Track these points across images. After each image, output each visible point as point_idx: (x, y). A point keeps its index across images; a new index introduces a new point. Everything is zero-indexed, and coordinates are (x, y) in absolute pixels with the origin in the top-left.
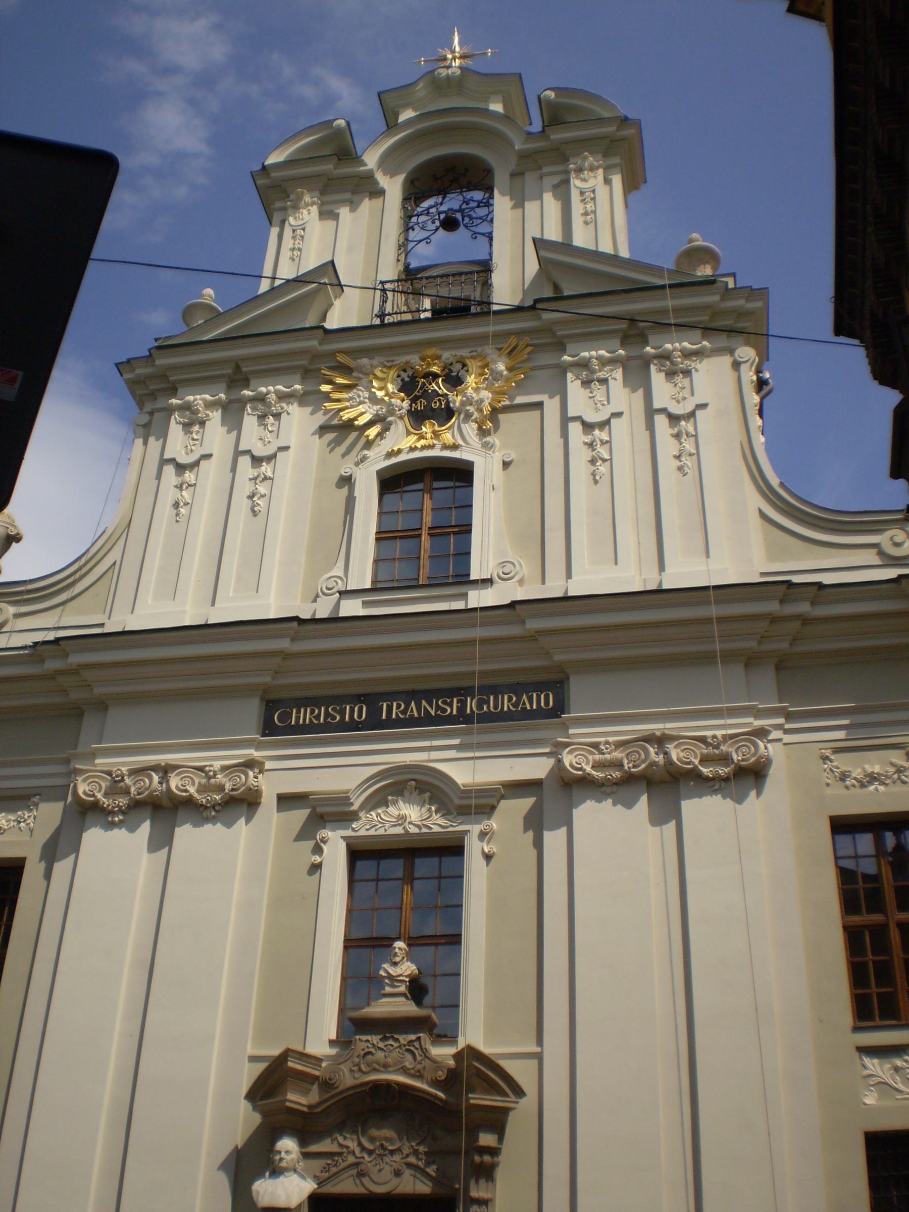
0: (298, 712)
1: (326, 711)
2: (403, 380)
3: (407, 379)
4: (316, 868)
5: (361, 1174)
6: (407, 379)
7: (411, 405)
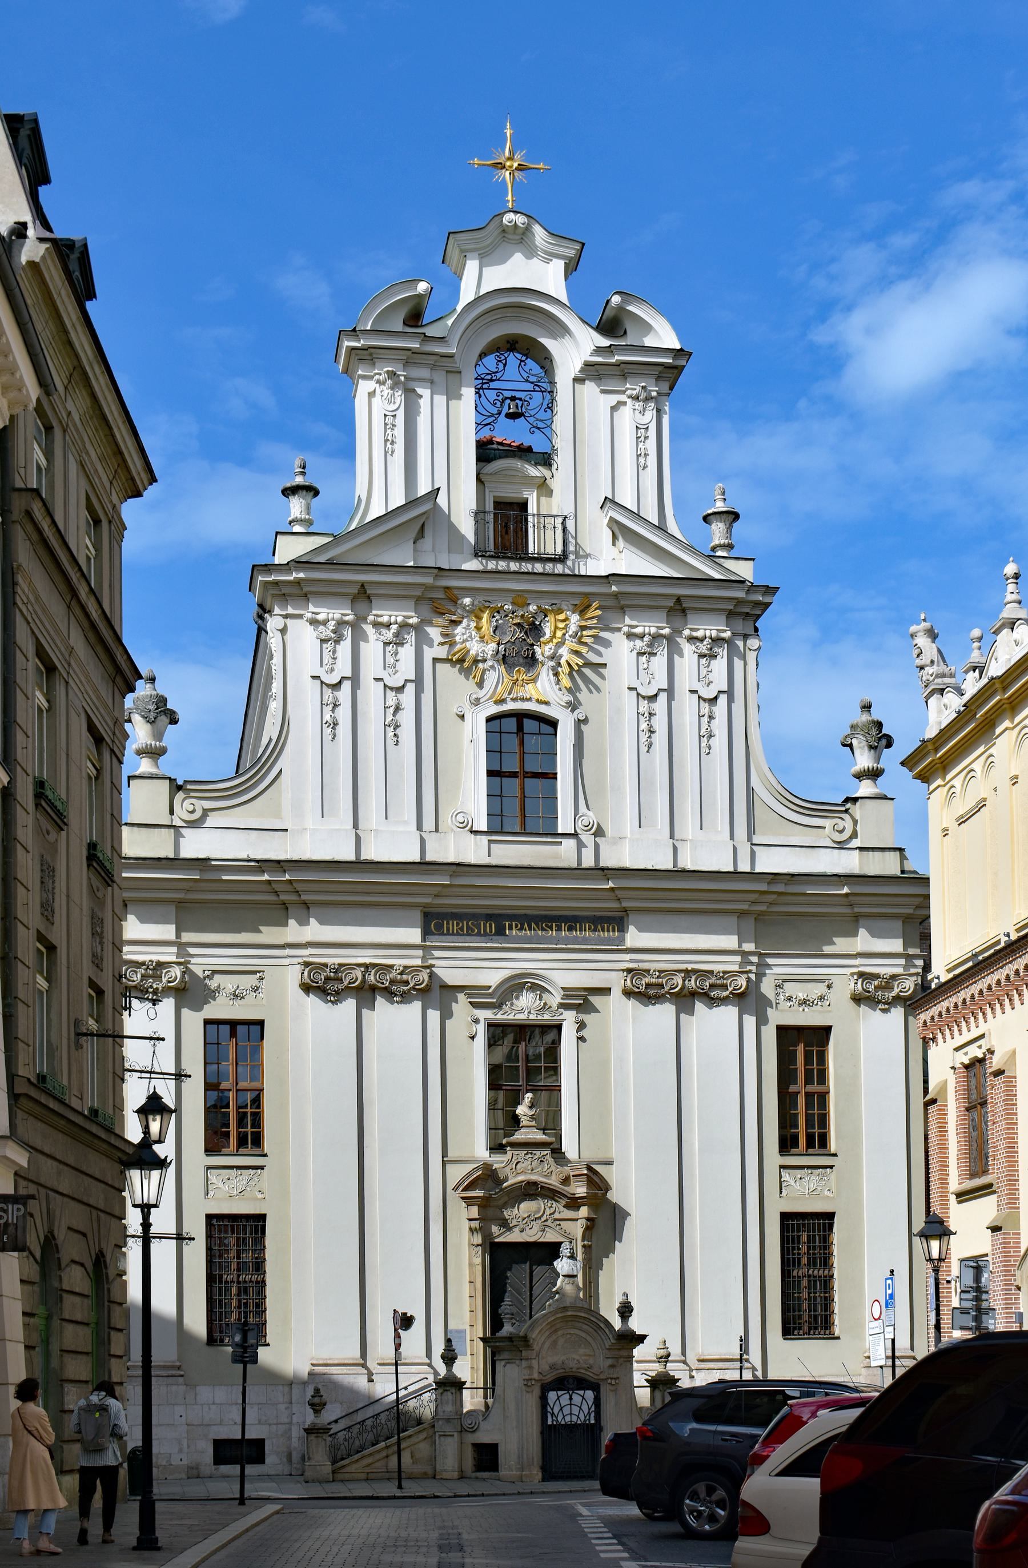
0: (448, 924)
1: (467, 924)
4: (473, 1038)
7: (505, 650)
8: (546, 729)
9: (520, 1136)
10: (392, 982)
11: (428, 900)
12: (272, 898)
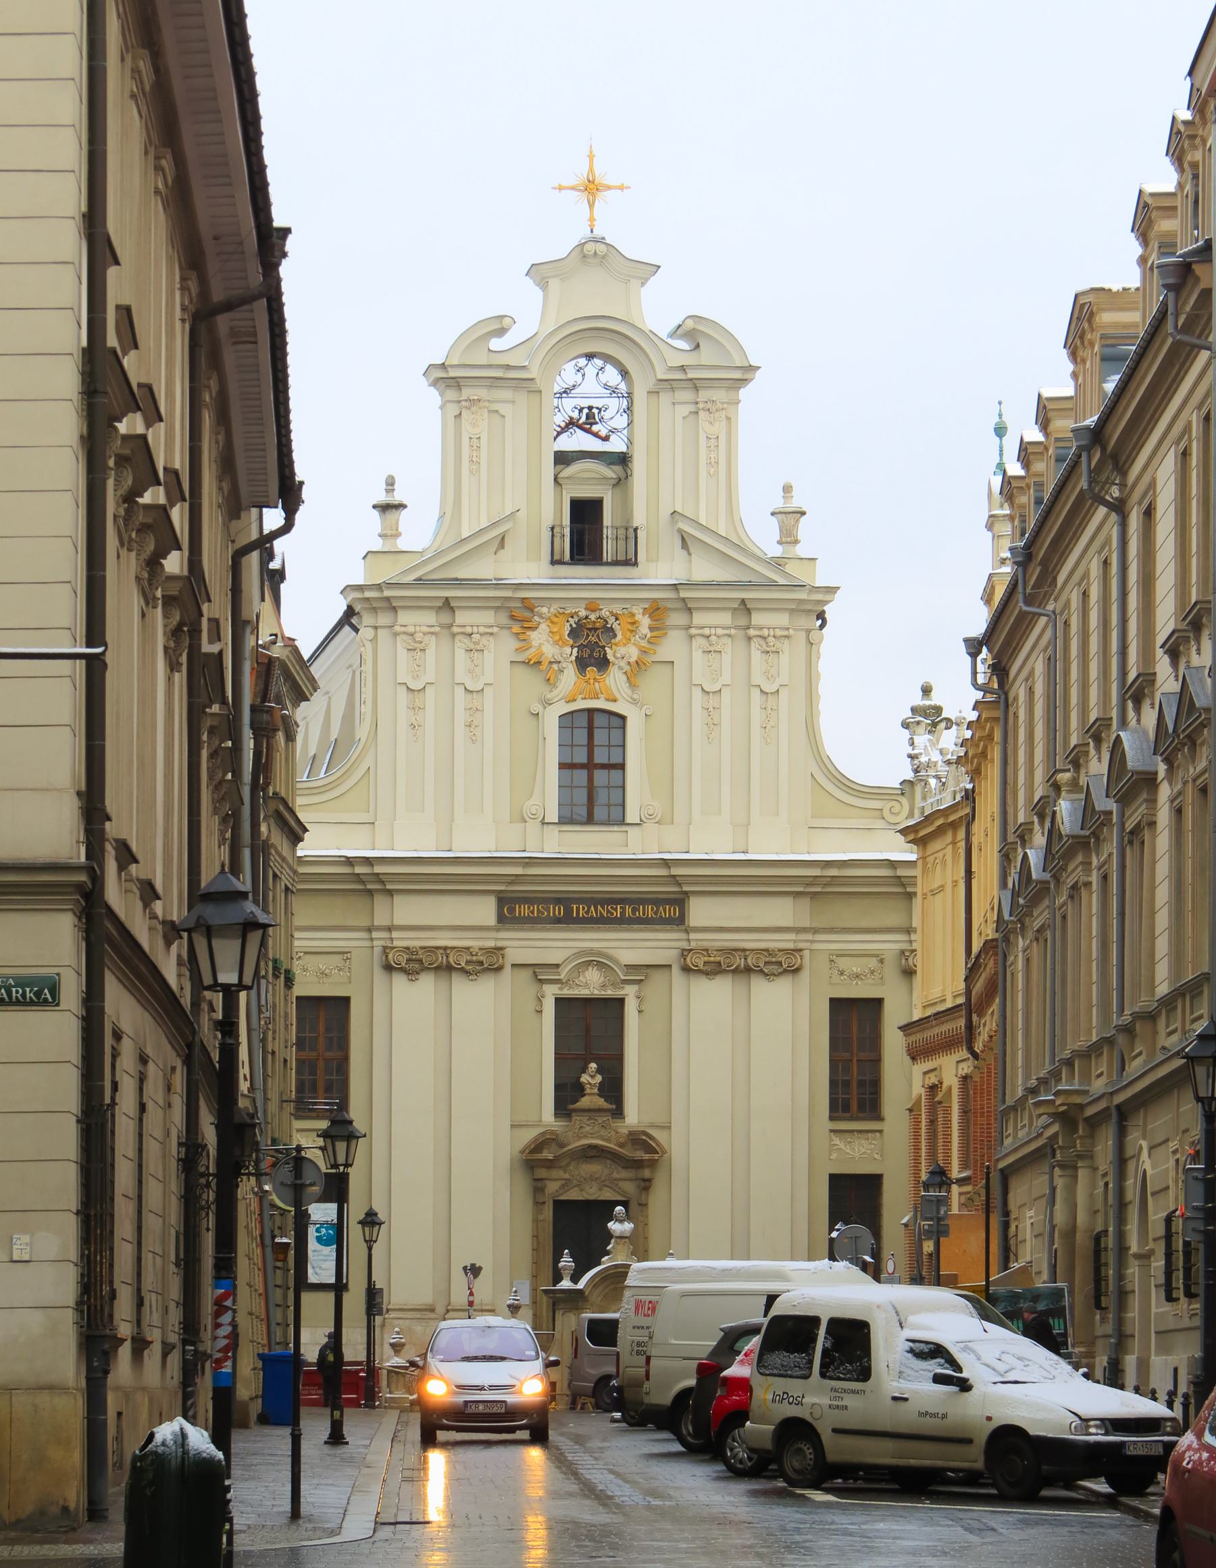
0: (520, 907)
2: (571, 625)
3: (574, 626)
5: (581, 1190)
6: (574, 626)
8: (615, 722)
9: (585, 1102)
10: (468, 962)
11: (503, 888)
12: (361, 887)
